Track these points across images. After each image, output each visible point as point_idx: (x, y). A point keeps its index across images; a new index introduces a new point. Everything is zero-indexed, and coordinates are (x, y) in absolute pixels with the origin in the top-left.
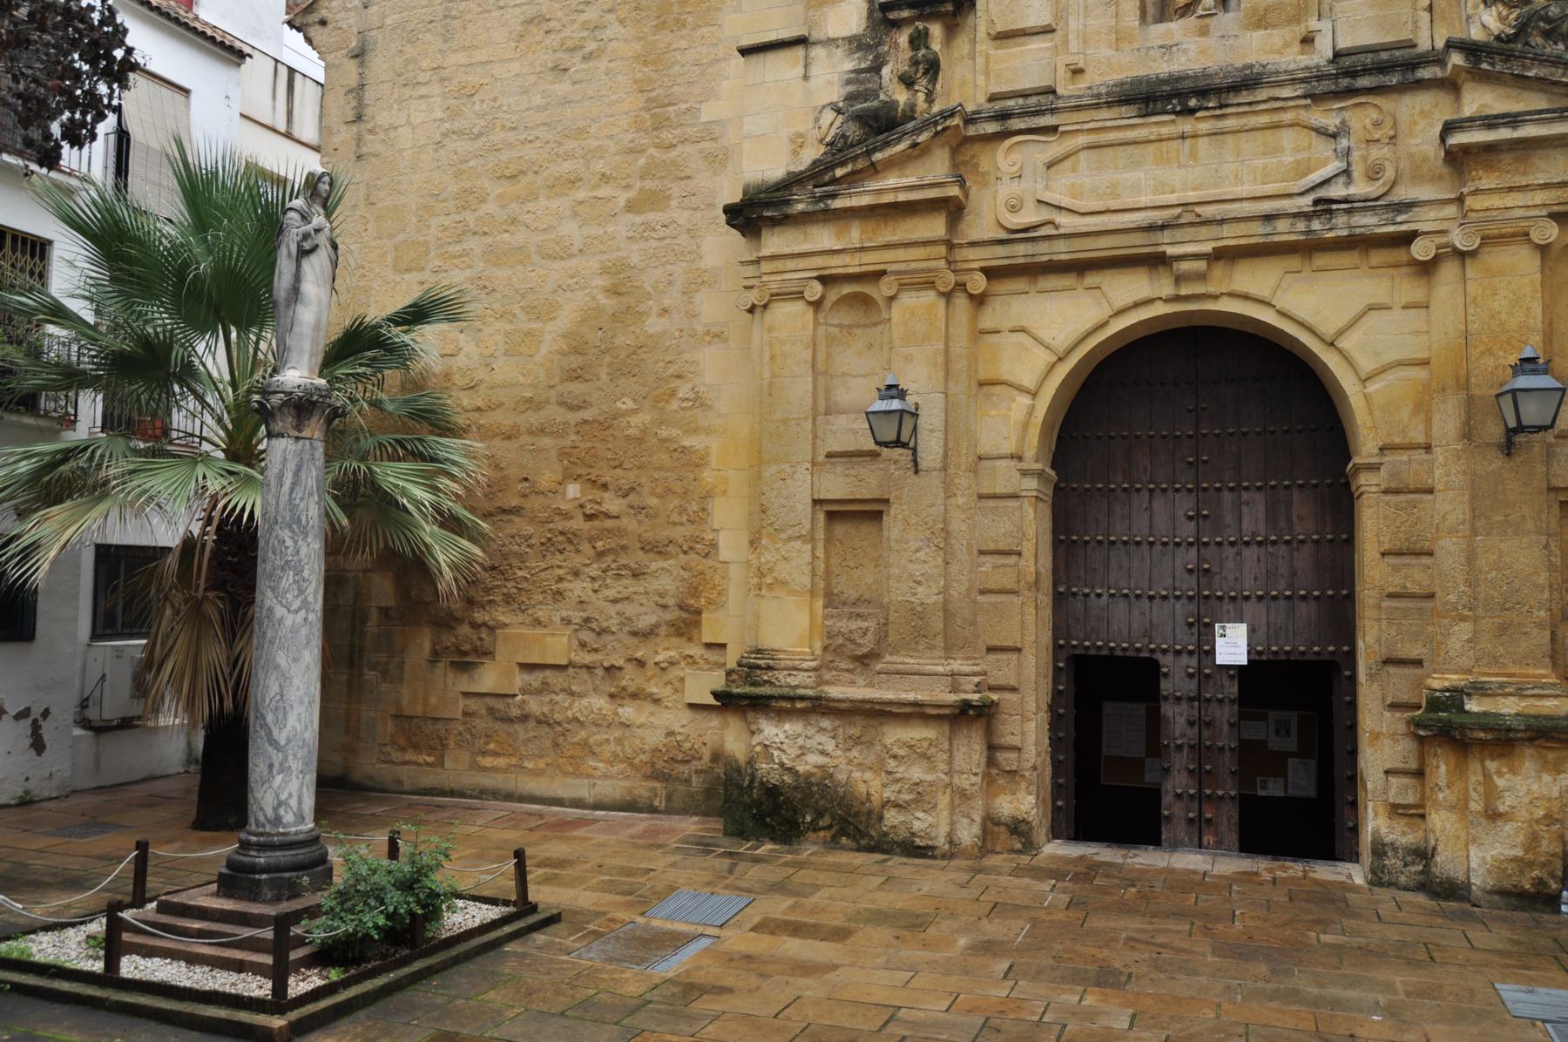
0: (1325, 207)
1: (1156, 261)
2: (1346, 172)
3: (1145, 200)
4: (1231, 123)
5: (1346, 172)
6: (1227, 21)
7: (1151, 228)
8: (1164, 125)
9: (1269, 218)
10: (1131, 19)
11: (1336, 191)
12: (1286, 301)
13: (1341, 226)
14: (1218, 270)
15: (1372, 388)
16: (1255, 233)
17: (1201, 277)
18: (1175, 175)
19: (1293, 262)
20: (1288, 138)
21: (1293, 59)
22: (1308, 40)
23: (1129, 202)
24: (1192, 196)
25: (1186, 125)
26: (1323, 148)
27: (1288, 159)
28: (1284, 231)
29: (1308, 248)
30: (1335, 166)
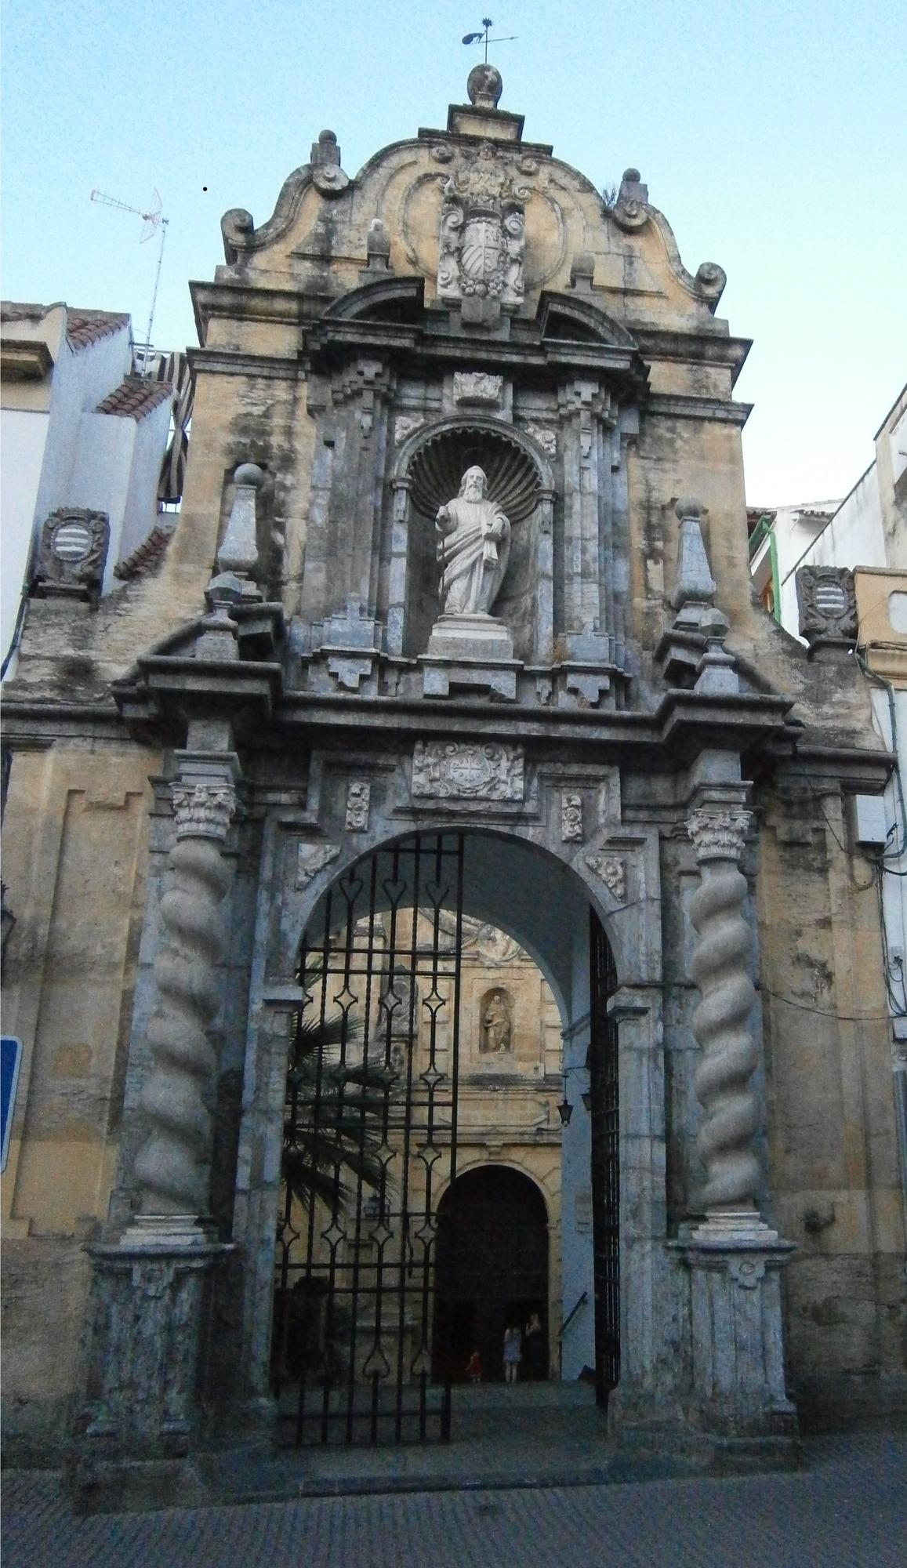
0: (540, 1131)
1: (482, 1146)
2: (548, 1120)
3: (480, 1122)
4: (510, 1096)
5: (548, 1120)
6: (508, 1057)
7: (482, 1134)
8: (485, 1094)
9: (522, 1134)
10: (476, 1051)
11: (544, 1126)
12: (527, 1164)
13: (545, 1139)
14: (505, 1151)
15: (555, 1198)
16: (516, 1139)
17: (498, 1153)
18: (490, 1114)
19: (529, 1149)
20: (529, 1105)
21: (530, 1075)
22: (536, 1068)
23: (473, 1122)
24: (495, 1123)
25: (495, 1095)
26: (541, 1111)
27: (529, 1112)
28: (527, 1139)
29: (536, 1145)
30: (544, 1117)
